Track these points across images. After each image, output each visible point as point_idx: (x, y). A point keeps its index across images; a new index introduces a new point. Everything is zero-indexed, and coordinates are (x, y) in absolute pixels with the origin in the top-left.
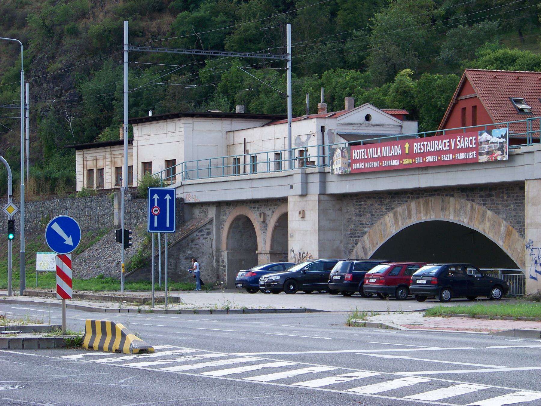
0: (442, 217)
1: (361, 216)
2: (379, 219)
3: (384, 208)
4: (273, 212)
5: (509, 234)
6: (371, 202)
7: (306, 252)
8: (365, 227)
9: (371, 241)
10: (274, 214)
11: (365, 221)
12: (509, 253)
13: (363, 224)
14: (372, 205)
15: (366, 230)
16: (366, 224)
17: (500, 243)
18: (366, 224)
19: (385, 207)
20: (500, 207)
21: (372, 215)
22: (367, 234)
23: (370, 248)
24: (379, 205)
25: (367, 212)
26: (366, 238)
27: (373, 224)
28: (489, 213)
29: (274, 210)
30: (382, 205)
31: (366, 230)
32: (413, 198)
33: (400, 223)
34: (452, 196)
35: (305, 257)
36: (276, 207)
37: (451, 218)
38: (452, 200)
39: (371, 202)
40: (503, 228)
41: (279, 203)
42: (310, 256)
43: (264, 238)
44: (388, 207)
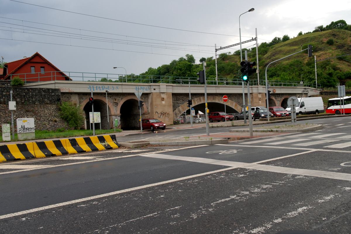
0: (214, 101)
1: (177, 101)
4: (122, 99)
5: (236, 105)
6: (182, 97)
10: (123, 99)
11: (179, 102)
12: (236, 110)
14: (183, 97)
15: (179, 105)
17: (233, 108)
20: (233, 99)
21: (183, 100)
22: (181, 106)
25: (181, 100)
26: (180, 108)
28: (229, 100)
31: (179, 105)
32: (202, 96)
33: (196, 103)
34: (217, 96)
35: (165, 114)
36: (124, 97)
37: (217, 101)
38: (217, 97)
39: (182, 97)
40: (234, 104)
43: (116, 109)
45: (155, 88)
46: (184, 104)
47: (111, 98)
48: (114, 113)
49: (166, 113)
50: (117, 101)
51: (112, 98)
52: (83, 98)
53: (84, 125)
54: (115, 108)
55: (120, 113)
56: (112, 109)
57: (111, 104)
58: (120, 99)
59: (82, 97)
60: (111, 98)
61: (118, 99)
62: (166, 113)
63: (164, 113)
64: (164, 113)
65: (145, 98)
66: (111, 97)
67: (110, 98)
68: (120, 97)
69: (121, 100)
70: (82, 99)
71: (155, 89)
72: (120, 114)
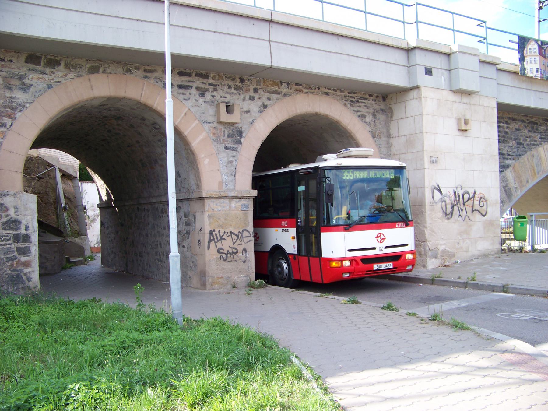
2: (530, 149)
3: (537, 137)
4: (265, 106)
7: (471, 192)
8: (507, 159)
9: (518, 178)
10: (269, 111)
13: (504, 154)
16: (509, 155)
18: (509, 155)
19: (539, 136)
21: (519, 144)
22: (511, 168)
23: (516, 188)
24: (529, 131)
25: (511, 139)
27: (520, 155)
29: (267, 102)
30: (535, 132)
35: (469, 199)
36: (274, 96)
39: (517, 127)
41: (284, 89)
42: (481, 198)
44: (543, 137)
45: (429, 64)
46: (521, 159)
47: (203, 95)
48: (220, 183)
49: (475, 193)
50: (234, 118)
51: (208, 96)
52: (27, 81)
53: (24, 259)
54: (225, 156)
55: (254, 187)
56: (207, 161)
57: (203, 135)
58: (254, 107)
59: (21, 78)
60: (203, 95)
61: (246, 105)
62: (475, 193)
63: (466, 196)
64: (466, 196)
65: (374, 116)
66: (207, 90)
67: (201, 100)
68: (252, 99)
69: (261, 112)
70: (25, 88)
71: (428, 72)
72: (255, 193)
